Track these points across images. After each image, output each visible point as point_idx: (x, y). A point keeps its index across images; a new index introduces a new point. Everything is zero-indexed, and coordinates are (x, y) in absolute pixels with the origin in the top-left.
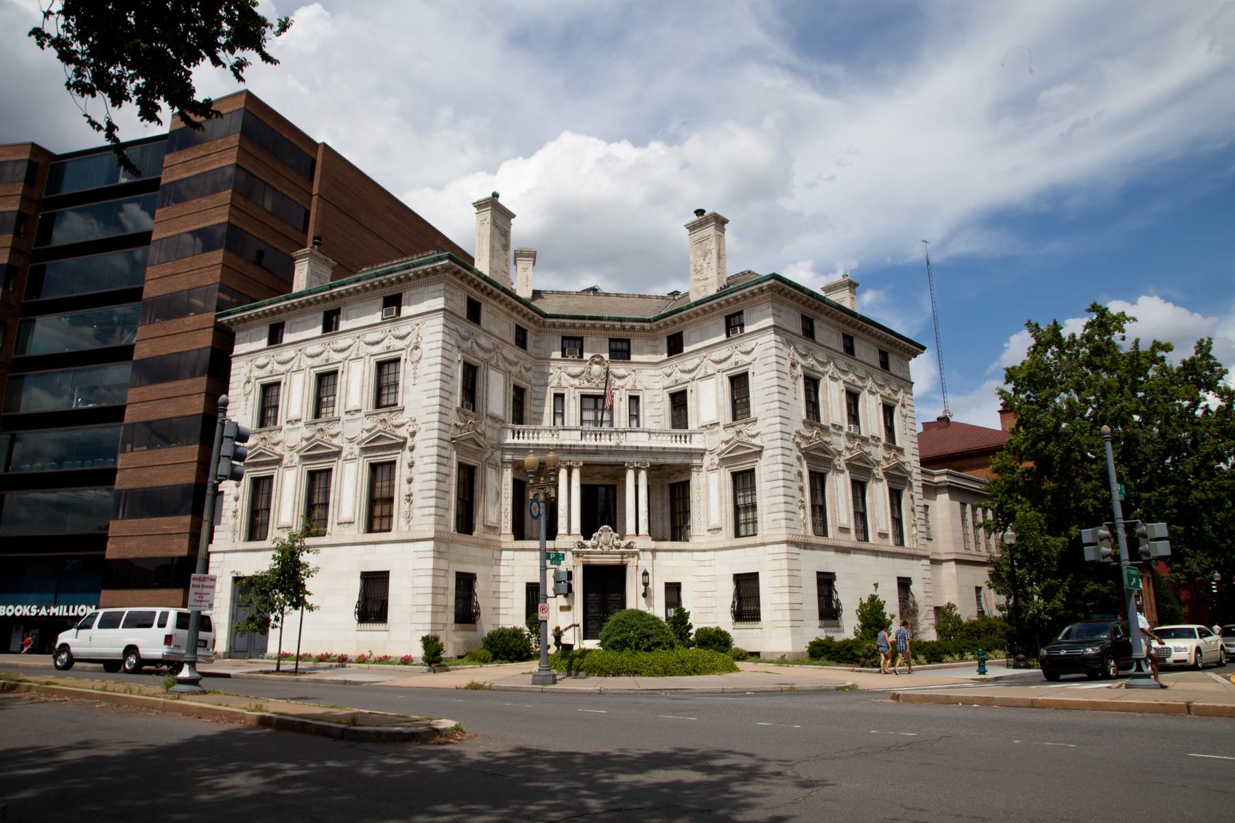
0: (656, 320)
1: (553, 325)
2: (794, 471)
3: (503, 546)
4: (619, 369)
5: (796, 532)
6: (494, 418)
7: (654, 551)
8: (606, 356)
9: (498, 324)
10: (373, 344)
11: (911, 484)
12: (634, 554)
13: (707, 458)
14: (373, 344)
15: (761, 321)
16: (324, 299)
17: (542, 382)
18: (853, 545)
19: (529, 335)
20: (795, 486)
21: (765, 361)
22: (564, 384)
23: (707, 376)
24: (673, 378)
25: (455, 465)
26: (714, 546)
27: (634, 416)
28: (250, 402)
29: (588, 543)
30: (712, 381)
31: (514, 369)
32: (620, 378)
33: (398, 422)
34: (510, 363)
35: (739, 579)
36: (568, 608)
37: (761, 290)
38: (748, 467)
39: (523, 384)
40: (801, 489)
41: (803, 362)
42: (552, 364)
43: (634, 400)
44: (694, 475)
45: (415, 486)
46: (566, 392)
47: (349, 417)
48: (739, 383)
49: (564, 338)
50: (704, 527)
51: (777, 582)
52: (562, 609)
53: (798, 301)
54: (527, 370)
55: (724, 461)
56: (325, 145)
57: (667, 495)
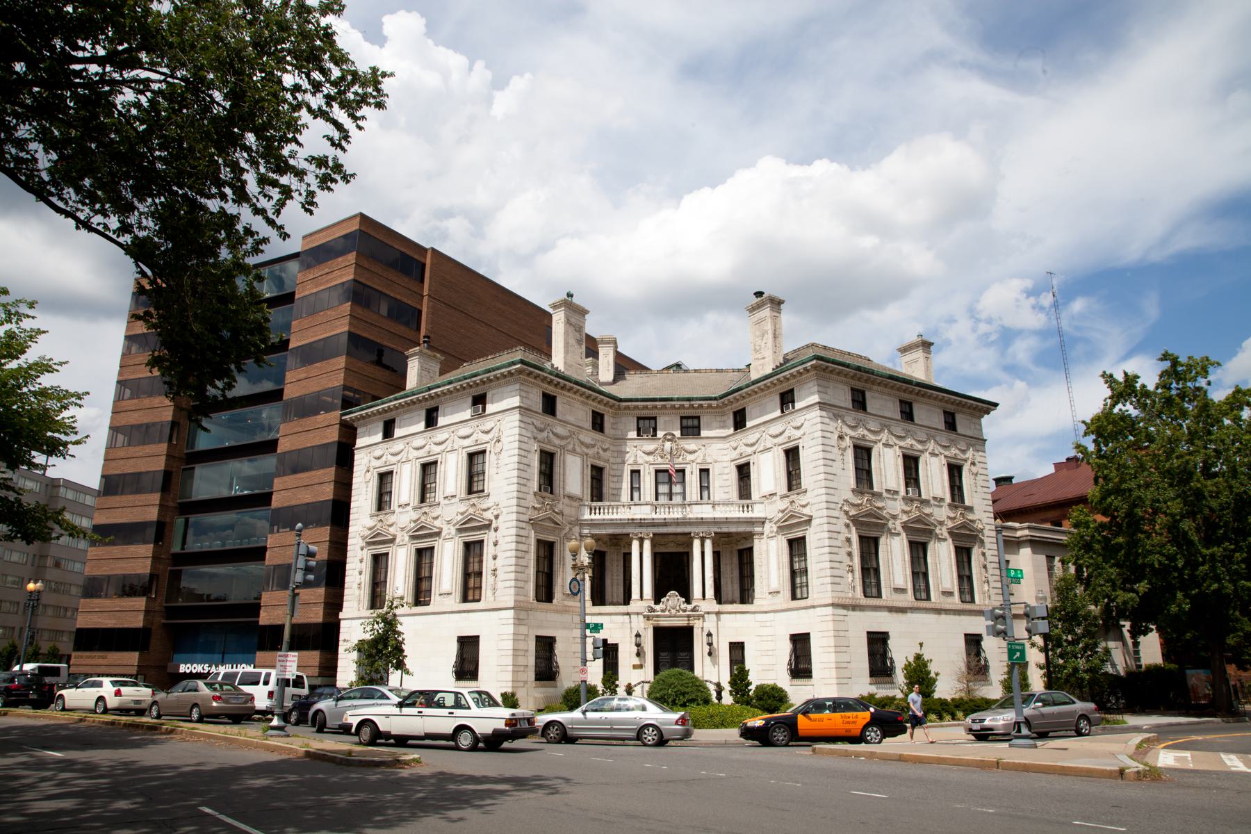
0: (721, 397)
1: (627, 408)
2: (842, 537)
4: (691, 444)
5: (843, 595)
6: (571, 497)
7: (718, 613)
8: (678, 433)
9: (574, 412)
10: (464, 438)
11: (982, 542)
12: (699, 617)
13: (767, 526)
14: (464, 438)
15: (808, 398)
16: (425, 399)
17: (619, 460)
18: (910, 605)
19: (606, 418)
20: (843, 552)
21: (811, 436)
22: (640, 461)
23: (767, 450)
24: (738, 451)
25: (533, 542)
27: (704, 487)
28: (370, 489)
29: (657, 607)
30: (769, 455)
31: (591, 452)
32: (691, 453)
33: (485, 506)
34: (588, 446)
36: (641, 666)
37: (806, 370)
39: (600, 464)
40: (850, 554)
41: (852, 433)
42: (629, 443)
43: (704, 472)
44: (756, 541)
45: (499, 562)
46: (641, 468)
47: (446, 501)
48: (792, 455)
49: (639, 419)
50: (766, 590)
52: (635, 667)
53: (846, 376)
54: (605, 450)
56: (433, 249)
57: (736, 560)
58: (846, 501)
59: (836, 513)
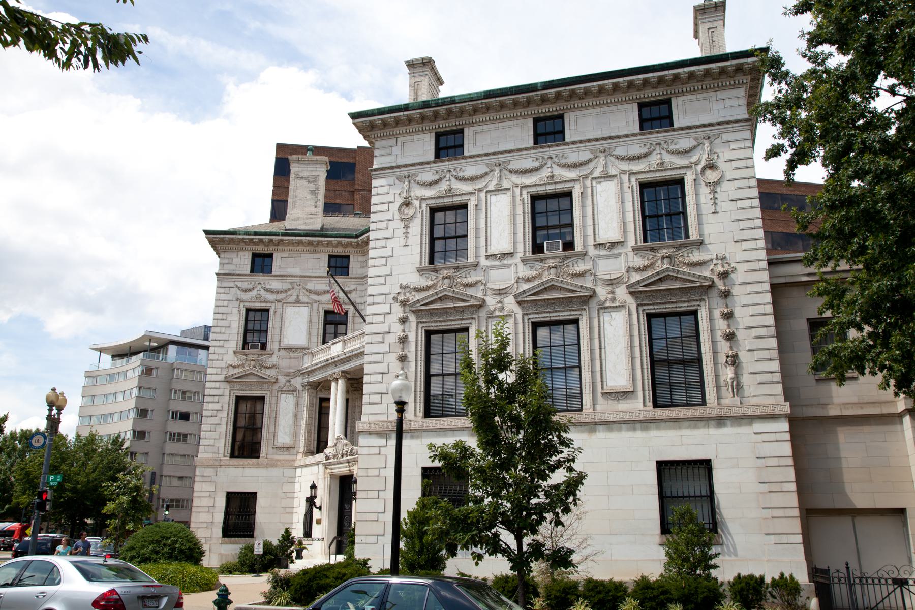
2: (393, 338)
3: (297, 464)
20: (392, 358)
58: (405, 287)
59: (385, 308)
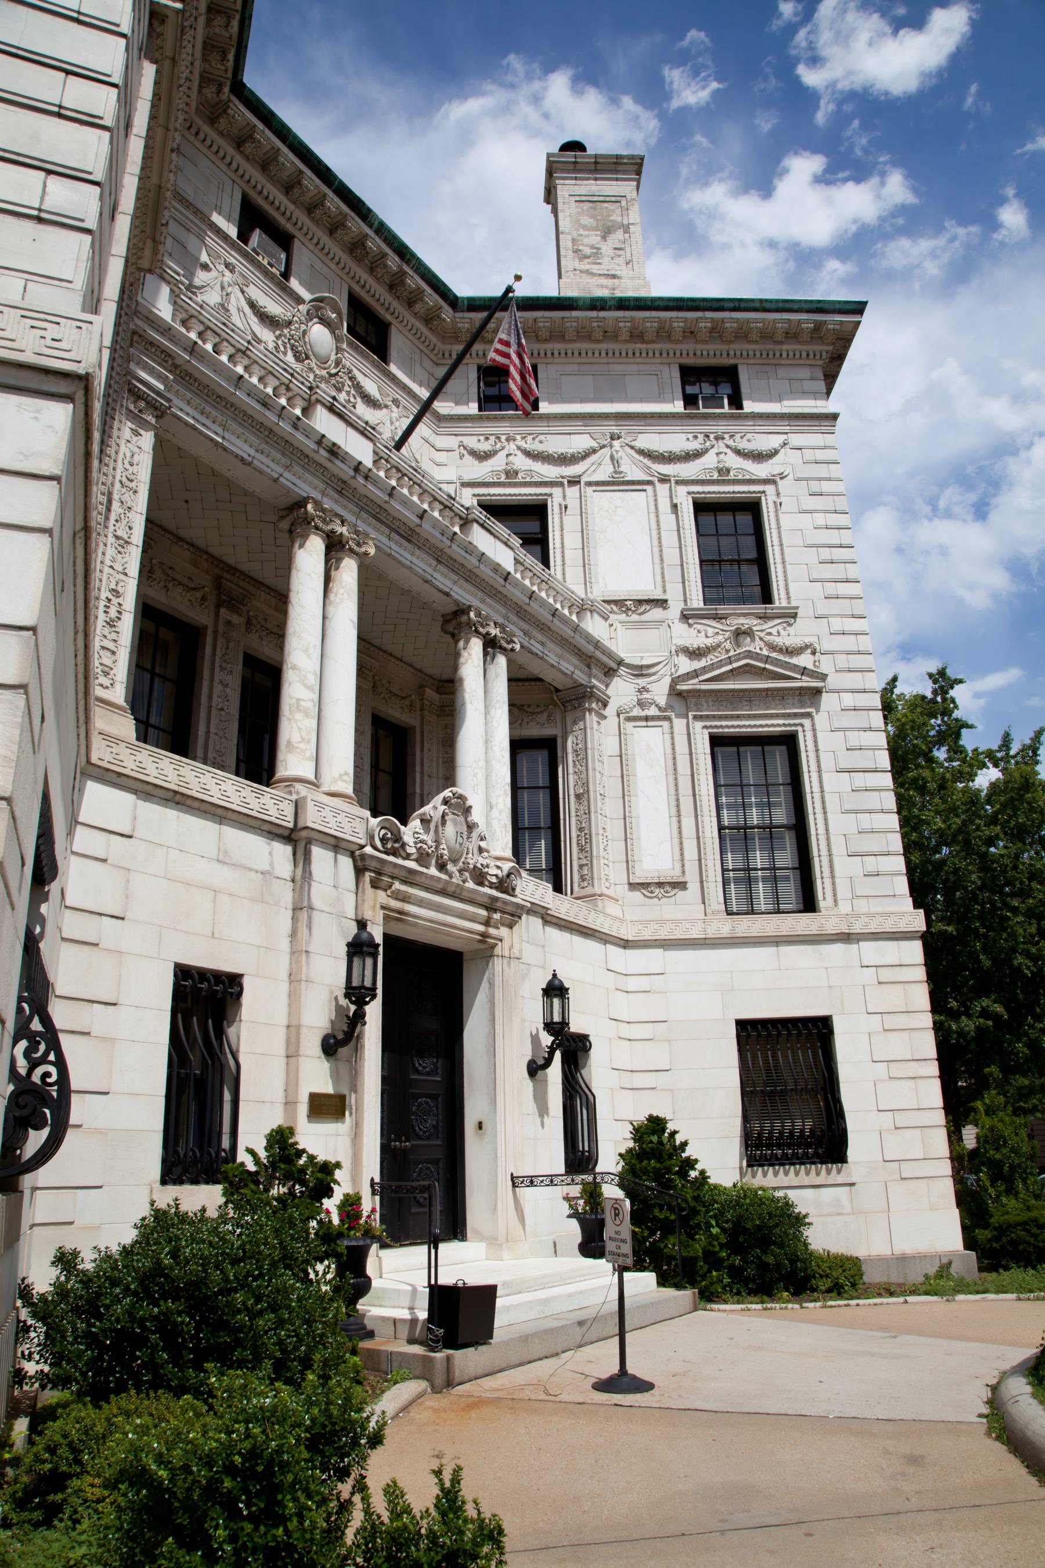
3: (100, 753)
24: (498, 463)
26: (663, 935)
30: (639, 500)
35: (753, 1034)
38: (774, 726)
44: (591, 719)
51: (897, 1046)
55: (683, 698)
